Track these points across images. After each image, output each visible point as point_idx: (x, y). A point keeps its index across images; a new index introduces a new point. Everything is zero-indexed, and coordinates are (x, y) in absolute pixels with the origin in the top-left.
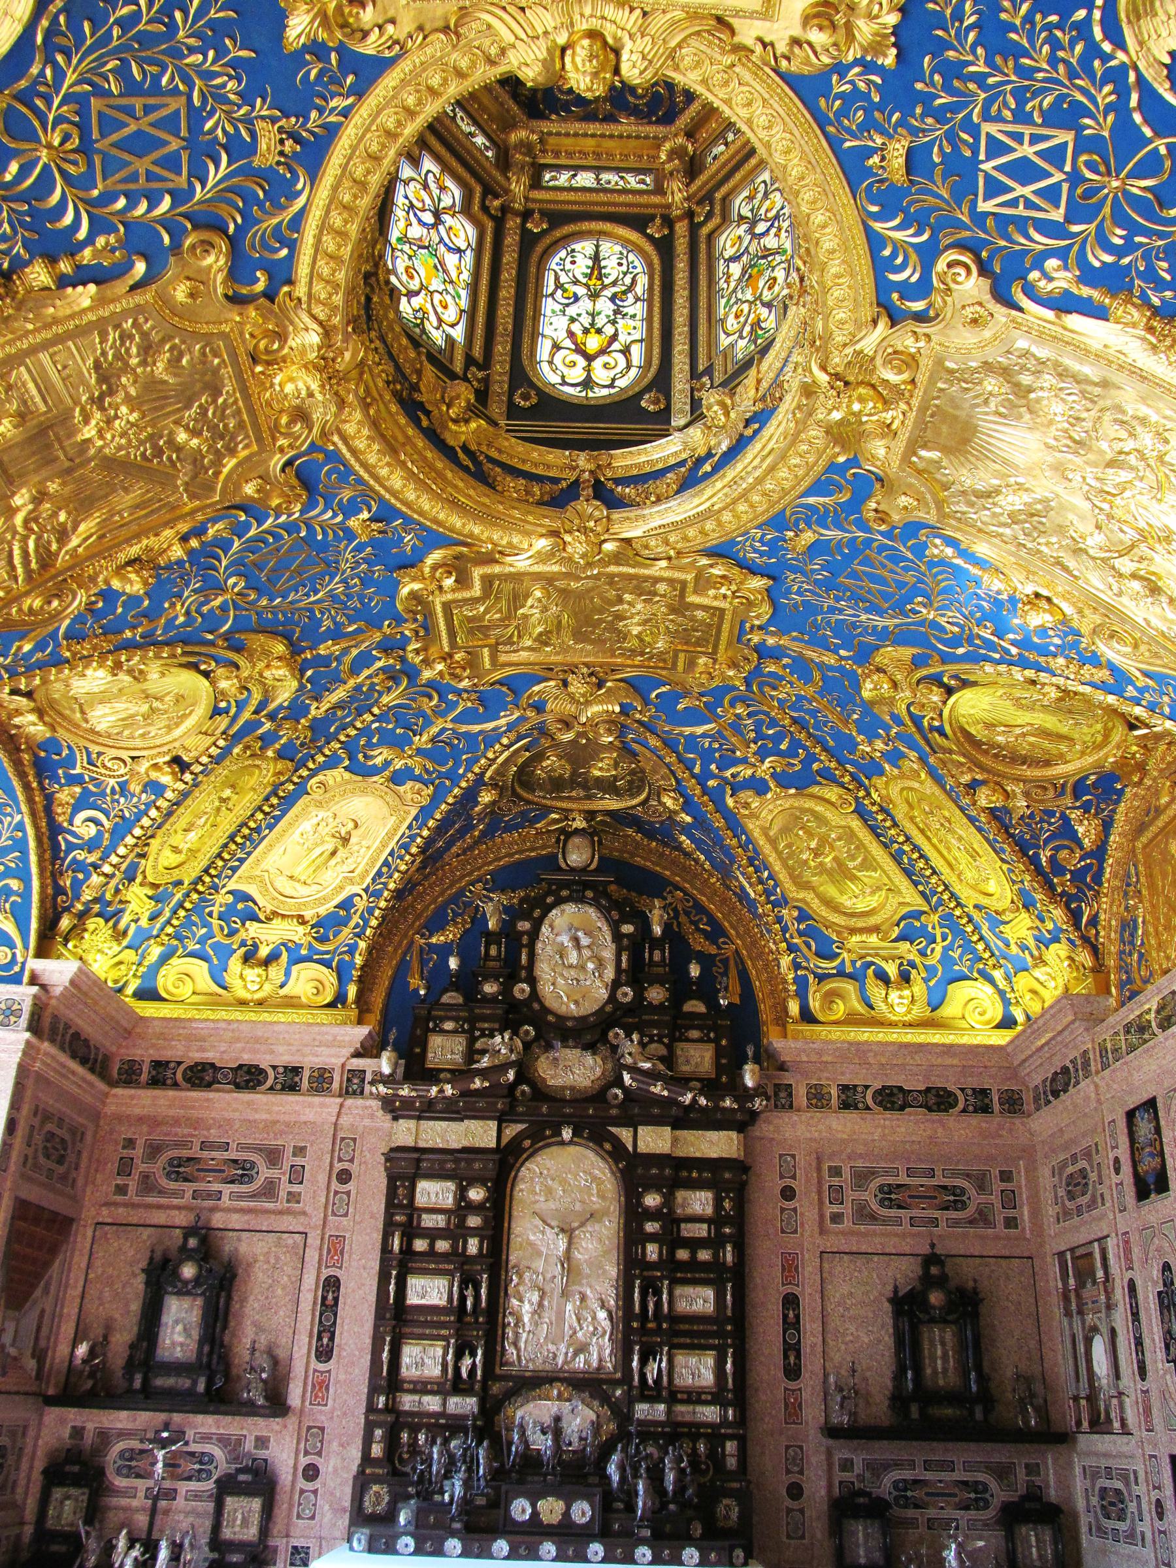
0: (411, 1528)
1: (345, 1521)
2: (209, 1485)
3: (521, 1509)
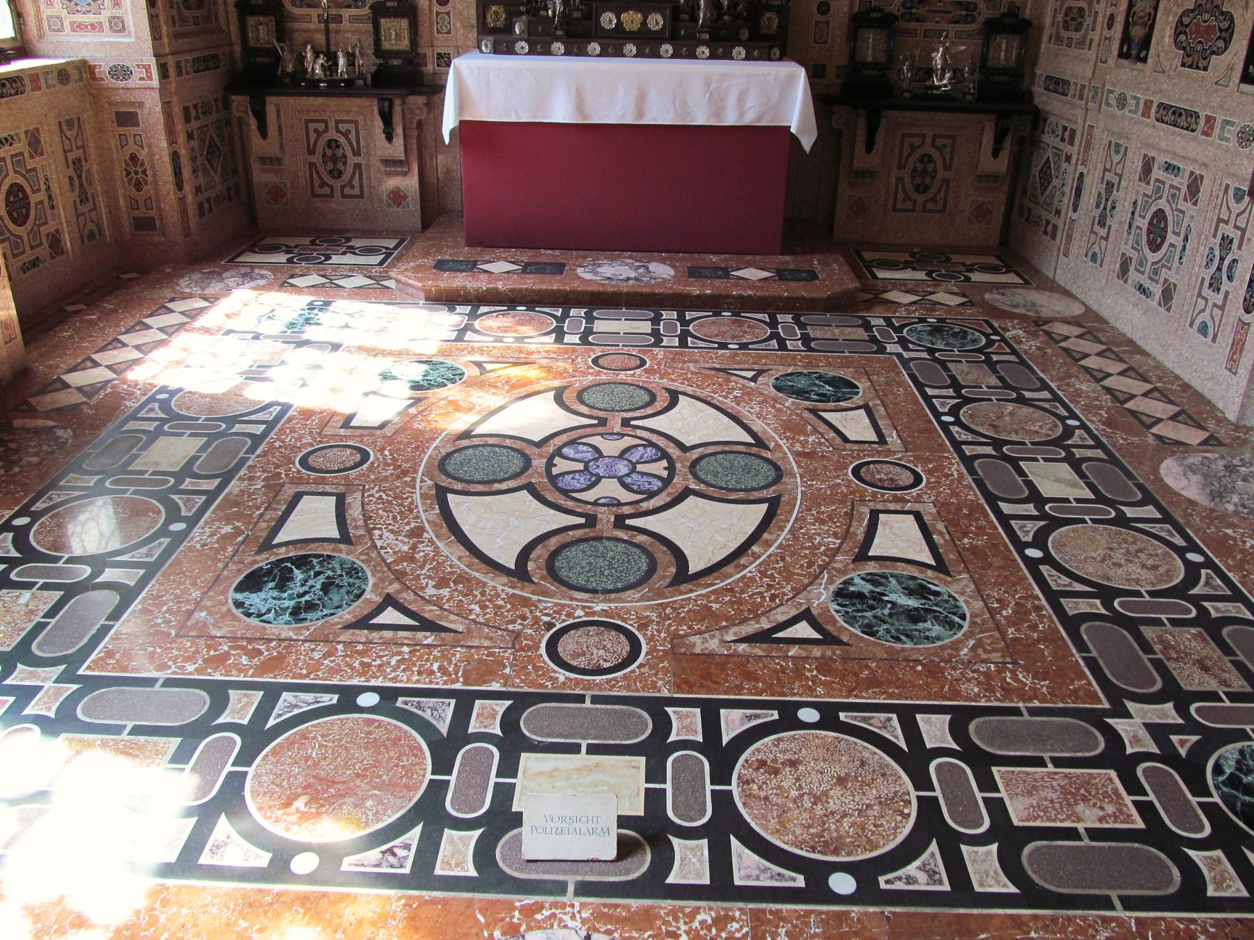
0: (526, 36)
1: (473, 35)
2: (366, 11)
3: (608, 20)
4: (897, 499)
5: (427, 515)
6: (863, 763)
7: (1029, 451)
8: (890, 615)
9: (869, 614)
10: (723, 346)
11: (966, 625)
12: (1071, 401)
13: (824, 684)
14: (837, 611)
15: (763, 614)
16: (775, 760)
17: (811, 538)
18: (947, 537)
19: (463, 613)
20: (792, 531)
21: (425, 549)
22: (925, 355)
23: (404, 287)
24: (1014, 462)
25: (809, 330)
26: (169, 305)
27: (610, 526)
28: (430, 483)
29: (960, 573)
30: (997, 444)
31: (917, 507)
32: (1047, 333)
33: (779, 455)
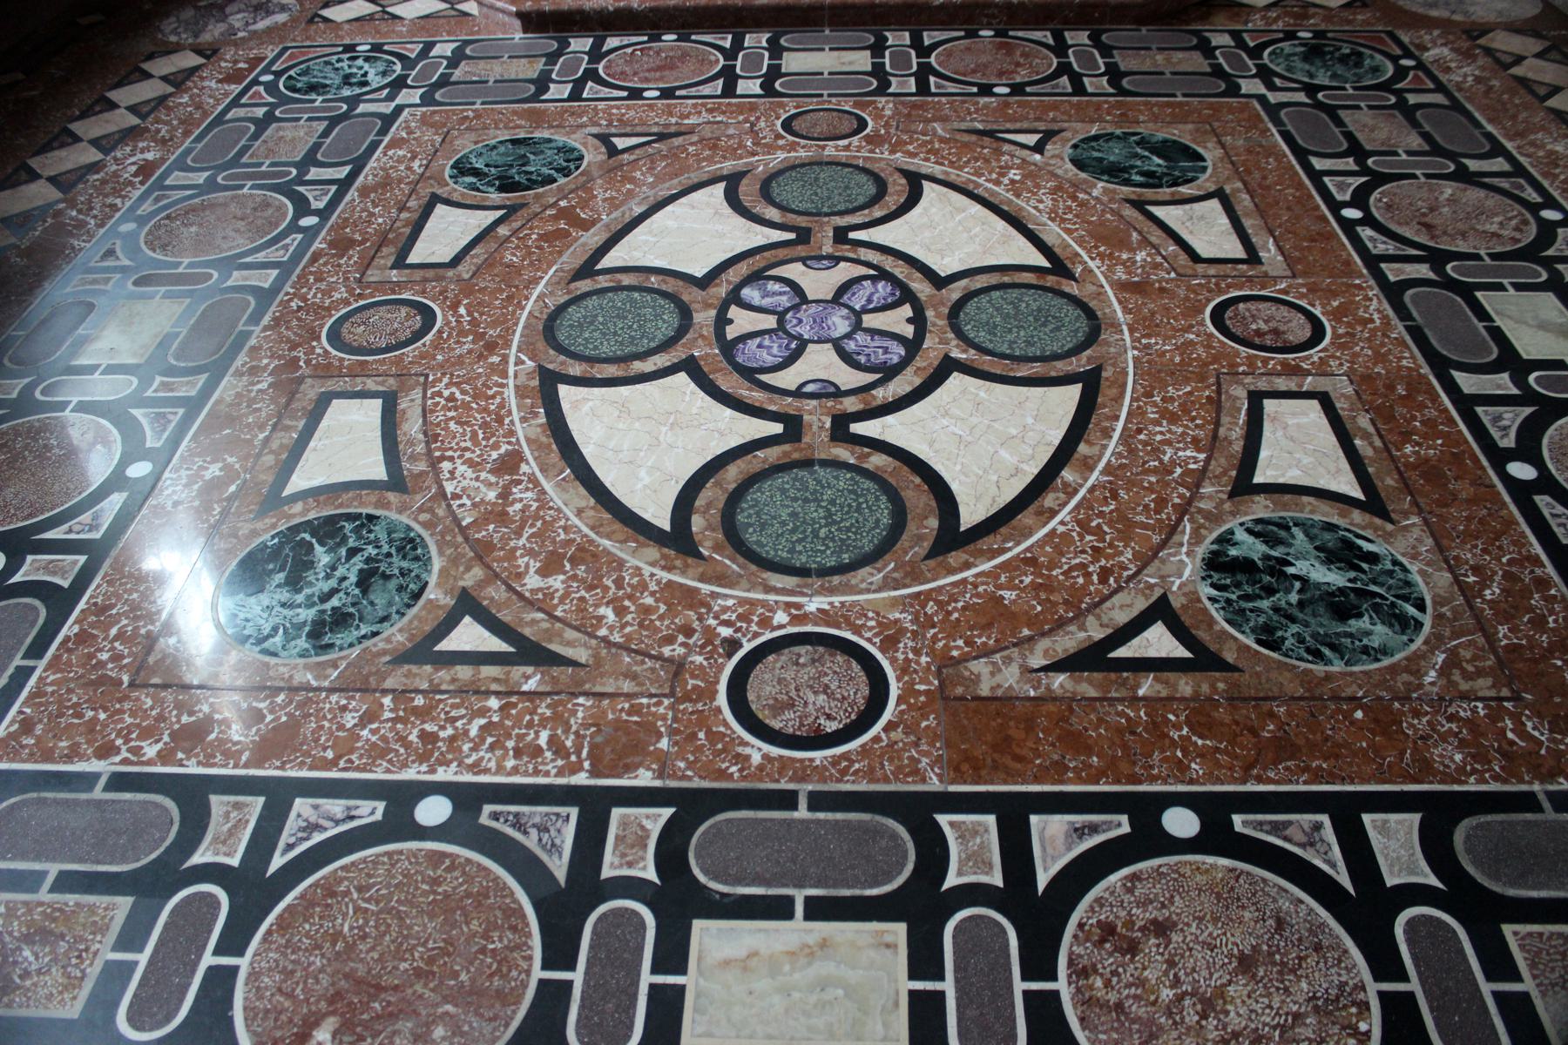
4: (1294, 371)
5: (526, 428)
6: (1281, 924)
7: (1487, 271)
8: (1301, 605)
9: (1265, 604)
10: (986, 90)
11: (1427, 620)
12: (1545, 175)
13: (1202, 754)
14: (1212, 599)
15: (1088, 610)
16: (1129, 924)
17: (1156, 451)
18: (1378, 443)
19: (586, 625)
20: (1126, 438)
21: (523, 496)
22: (1301, 97)
23: (491, 12)
24: (1466, 291)
25: (1117, 57)
26: (146, 66)
27: (825, 436)
28: (530, 364)
29: (1406, 515)
30: (1437, 258)
31: (1323, 384)
32: (1488, 51)
33: (1092, 288)
